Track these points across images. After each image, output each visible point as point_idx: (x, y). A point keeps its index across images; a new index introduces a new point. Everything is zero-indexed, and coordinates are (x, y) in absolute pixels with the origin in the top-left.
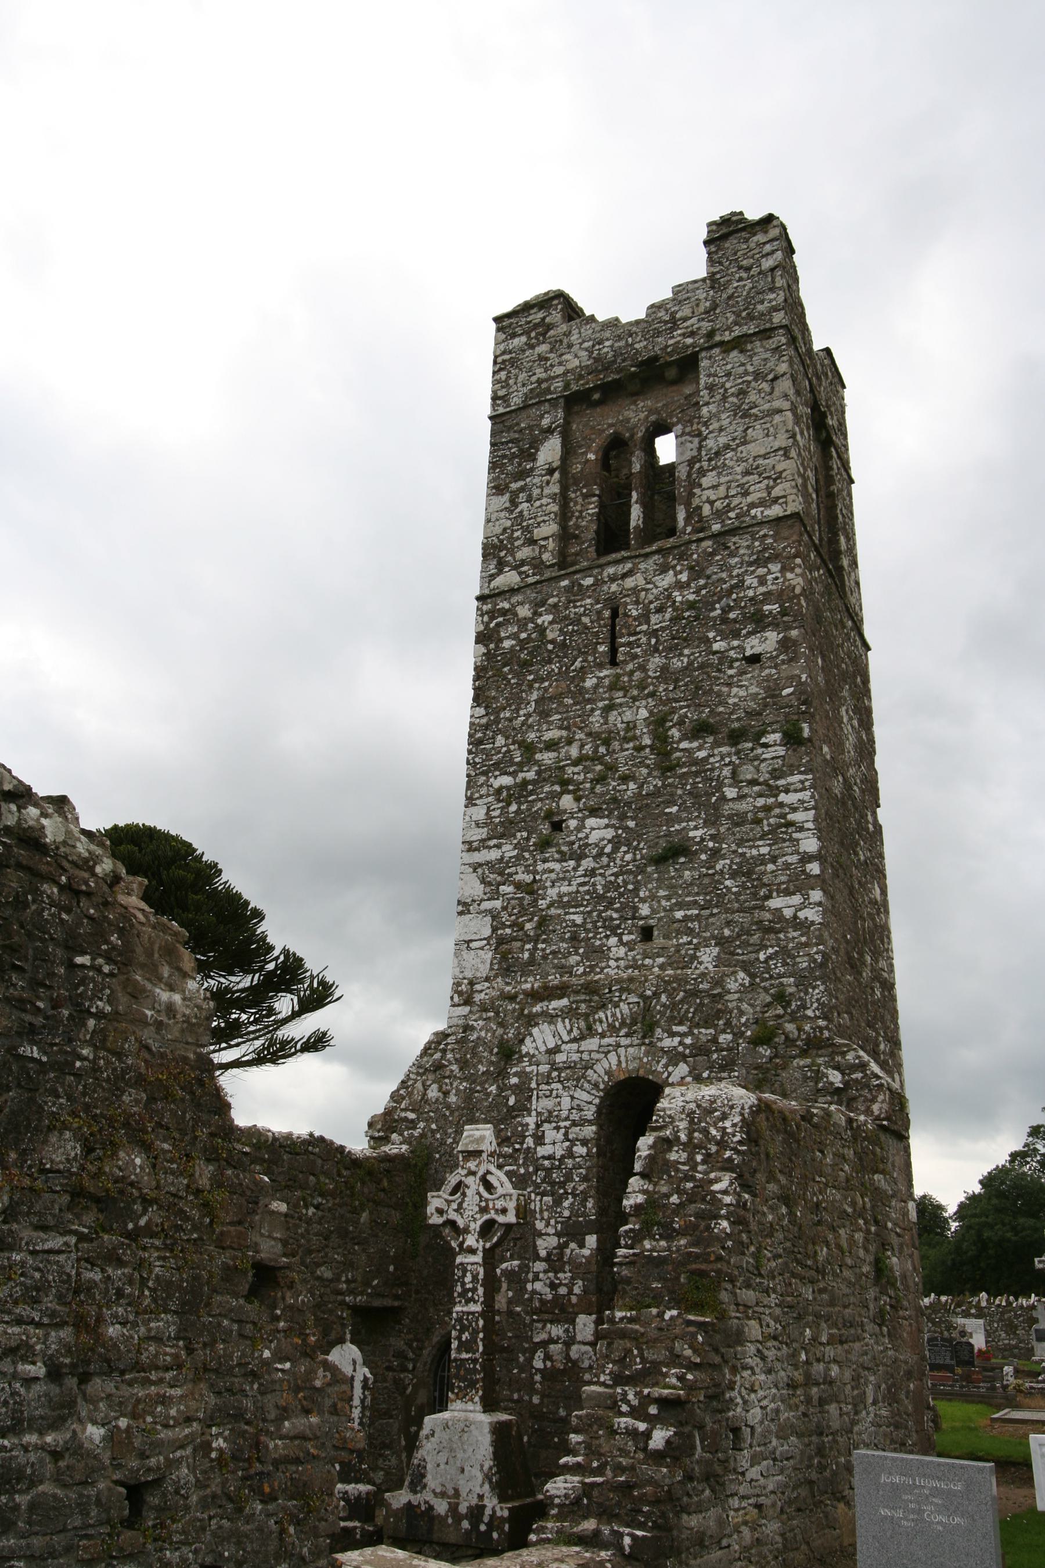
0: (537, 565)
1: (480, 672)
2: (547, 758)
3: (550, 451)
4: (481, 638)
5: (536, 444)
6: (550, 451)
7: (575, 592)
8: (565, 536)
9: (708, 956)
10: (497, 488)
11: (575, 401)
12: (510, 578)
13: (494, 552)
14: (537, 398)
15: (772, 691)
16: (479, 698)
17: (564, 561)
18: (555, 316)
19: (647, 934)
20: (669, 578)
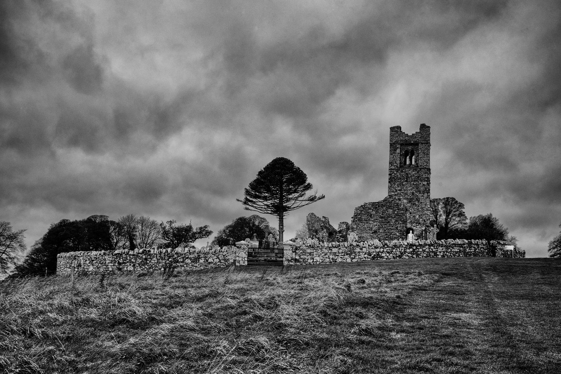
0: (397, 167)
1: (389, 179)
2: (399, 192)
3: (398, 151)
4: (390, 175)
5: (396, 149)
6: (398, 151)
7: (402, 171)
8: (400, 163)
9: (417, 216)
10: (391, 154)
11: (401, 145)
12: (393, 167)
13: (391, 163)
14: (397, 142)
15: (426, 189)
16: (389, 182)
17: (400, 167)
18: (399, 130)
19: (411, 213)
20: (414, 173)
